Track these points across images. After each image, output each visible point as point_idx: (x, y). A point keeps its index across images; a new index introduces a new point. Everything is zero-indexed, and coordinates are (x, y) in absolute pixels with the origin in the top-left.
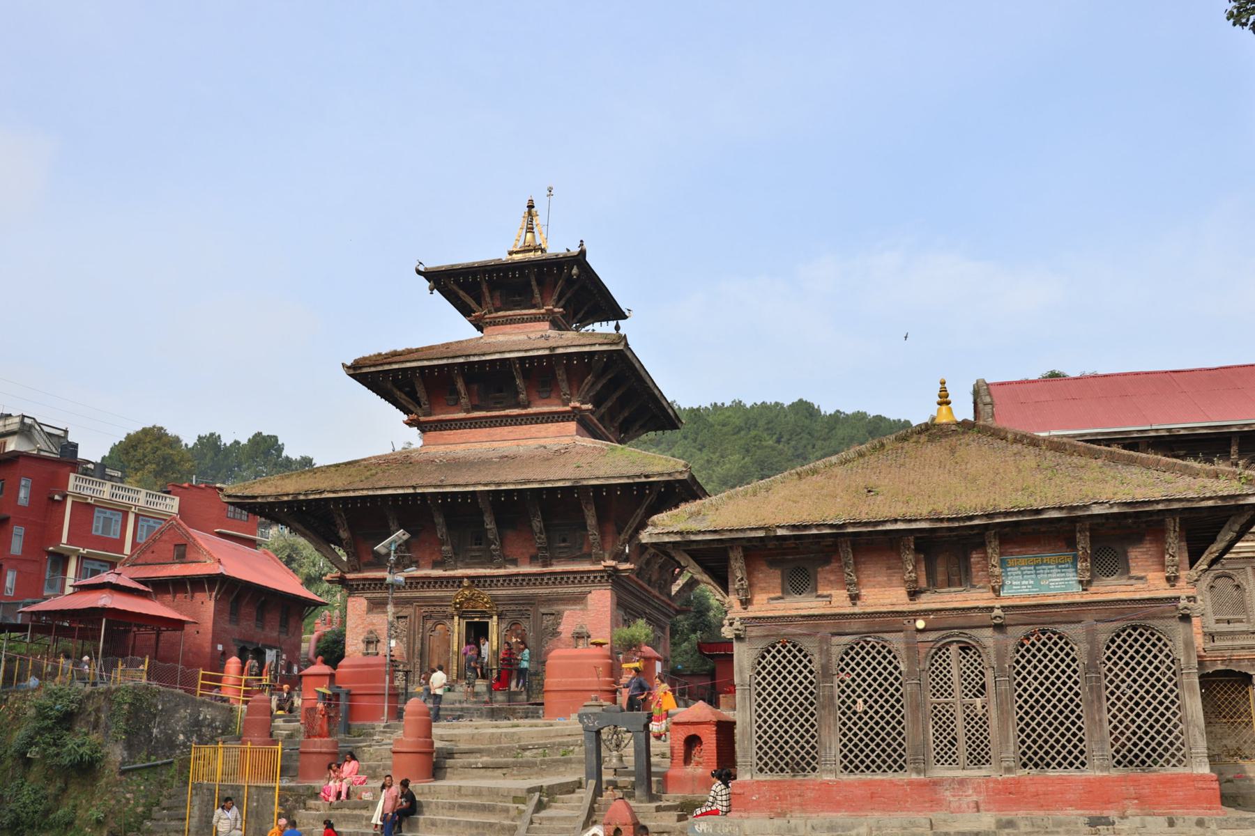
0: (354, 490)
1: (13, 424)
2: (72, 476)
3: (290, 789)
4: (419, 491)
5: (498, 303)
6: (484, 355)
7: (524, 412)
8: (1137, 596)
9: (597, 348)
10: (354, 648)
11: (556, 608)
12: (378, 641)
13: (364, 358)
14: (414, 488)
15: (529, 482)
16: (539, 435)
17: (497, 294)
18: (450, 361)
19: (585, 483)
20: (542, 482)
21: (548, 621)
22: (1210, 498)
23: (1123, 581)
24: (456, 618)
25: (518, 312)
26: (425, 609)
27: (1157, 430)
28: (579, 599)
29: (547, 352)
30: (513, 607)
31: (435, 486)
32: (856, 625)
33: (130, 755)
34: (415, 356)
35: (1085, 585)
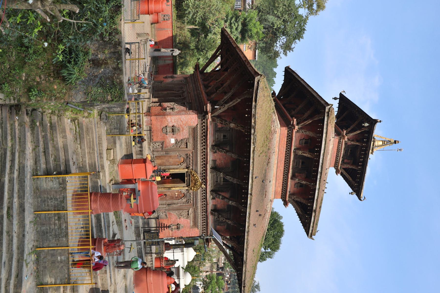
0: (253, 162)
4: (249, 196)
6: (320, 181)
7: (289, 180)
10: (169, 120)
11: (191, 216)
12: (173, 134)
14: (251, 194)
15: (247, 245)
16: (278, 182)
18: (320, 164)
19: (244, 265)
20: (247, 250)
21: (185, 213)
24: (187, 170)
25: (342, 153)
26: (191, 155)
28: (195, 224)
29: (314, 208)
30: (192, 196)
31: (250, 204)
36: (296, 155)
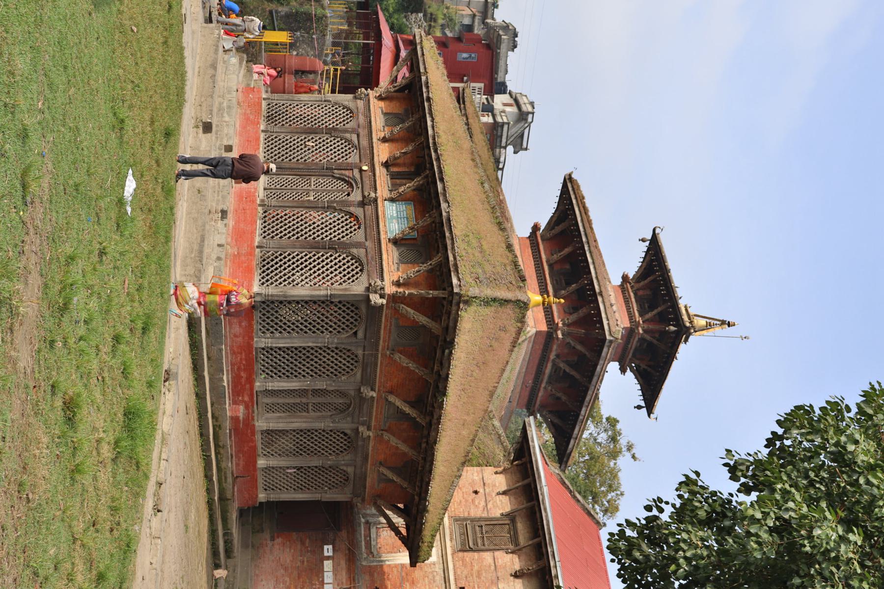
1: (527, 108)
2: (482, 85)
3: (260, 49)
5: (640, 293)
6: (590, 252)
8: (384, 263)
9: (605, 322)
13: (579, 186)
17: (648, 292)
18: (583, 233)
22: (455, 258)
23: (396, 261)
27: (556, 567)
29: (597, 290)
32: (364, 142)
33: (282, 17)
34: (587, 225)
35: (395, 242)
36: (551, 266)
